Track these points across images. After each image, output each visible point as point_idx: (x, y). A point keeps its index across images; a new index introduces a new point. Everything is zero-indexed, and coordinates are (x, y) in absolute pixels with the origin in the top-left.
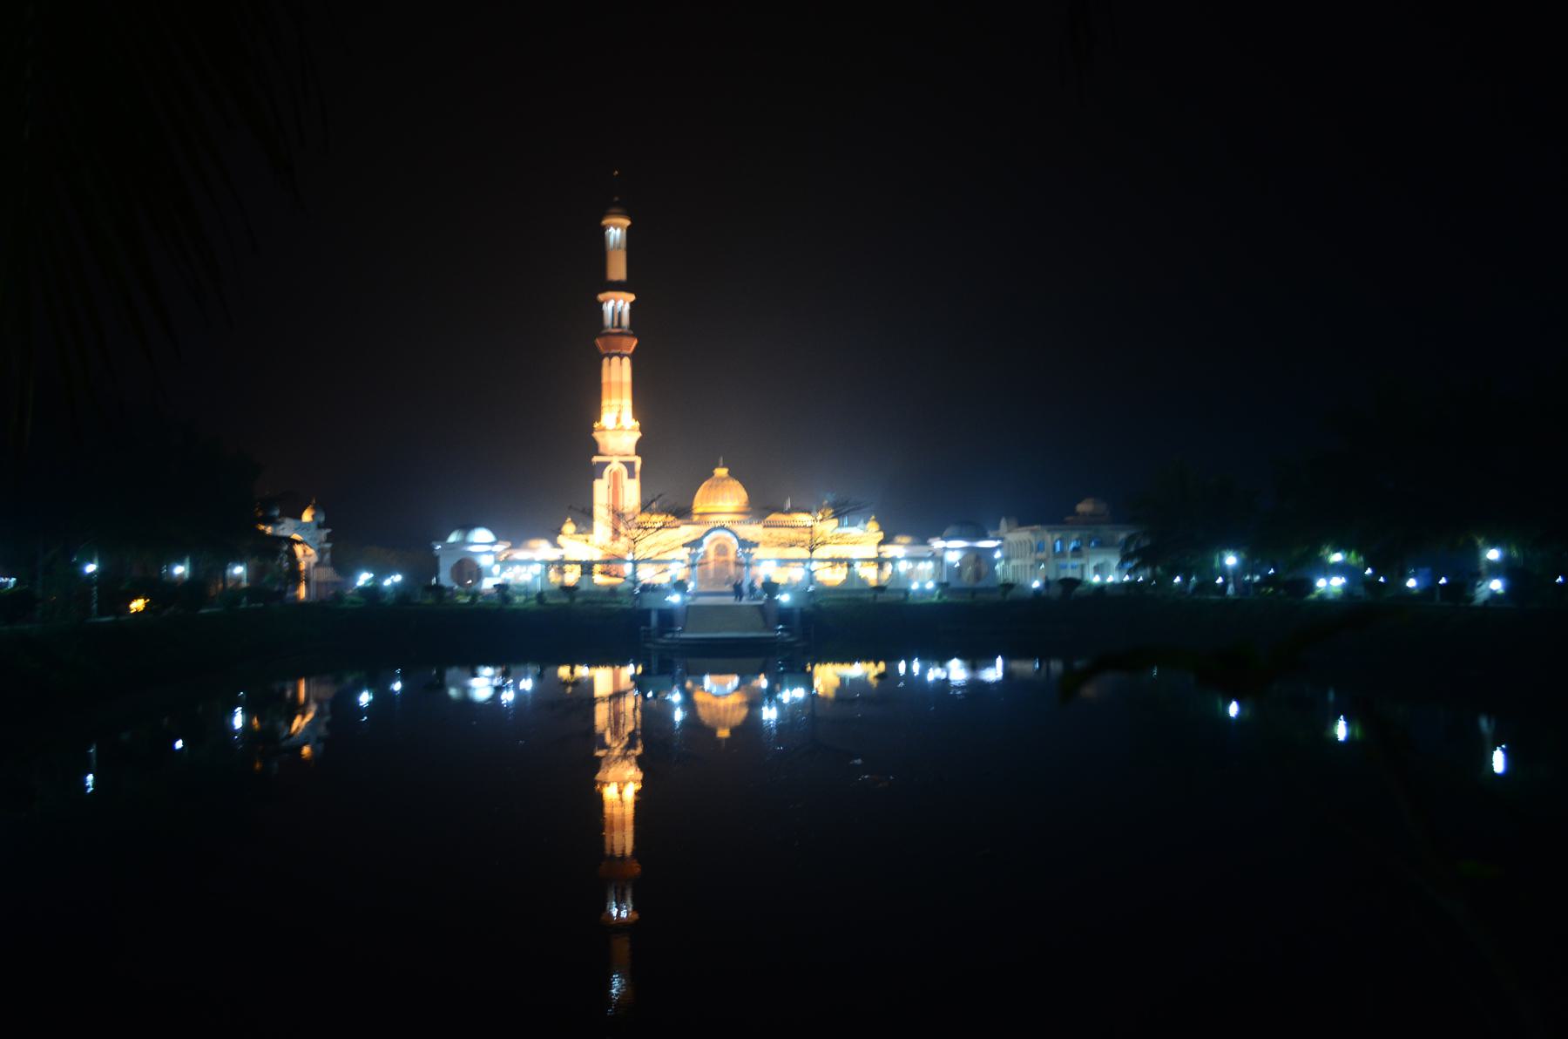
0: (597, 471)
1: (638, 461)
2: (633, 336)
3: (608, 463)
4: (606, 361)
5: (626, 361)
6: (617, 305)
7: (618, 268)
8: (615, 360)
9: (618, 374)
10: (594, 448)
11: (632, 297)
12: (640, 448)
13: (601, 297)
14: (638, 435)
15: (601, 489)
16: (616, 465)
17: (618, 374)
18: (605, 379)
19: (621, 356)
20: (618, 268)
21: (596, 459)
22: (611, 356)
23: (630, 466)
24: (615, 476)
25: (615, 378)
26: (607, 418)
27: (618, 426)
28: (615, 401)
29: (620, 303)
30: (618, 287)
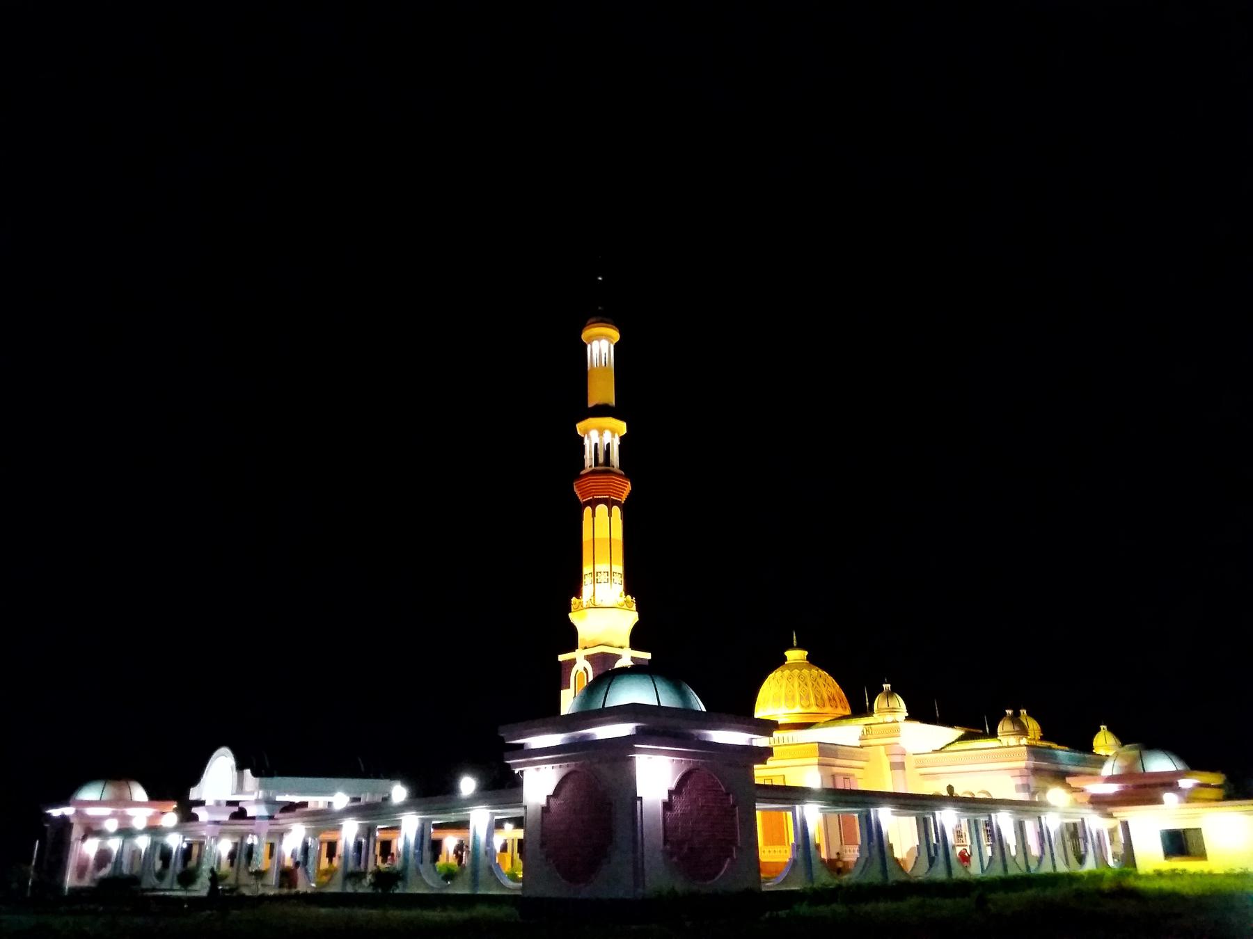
2: (627, 476)
4: (588, 510)
5: (616, 510)
6: (602, 436)
8: (602, 509)
9: (603, 530)
11: (622, 427)
13: (580, 427)
14: (633, 617)
17: (603, 530)
19: (610, 503)
22: (593, 504)
25: (602, 533)
29: (607, 434)
30: (602, 411)
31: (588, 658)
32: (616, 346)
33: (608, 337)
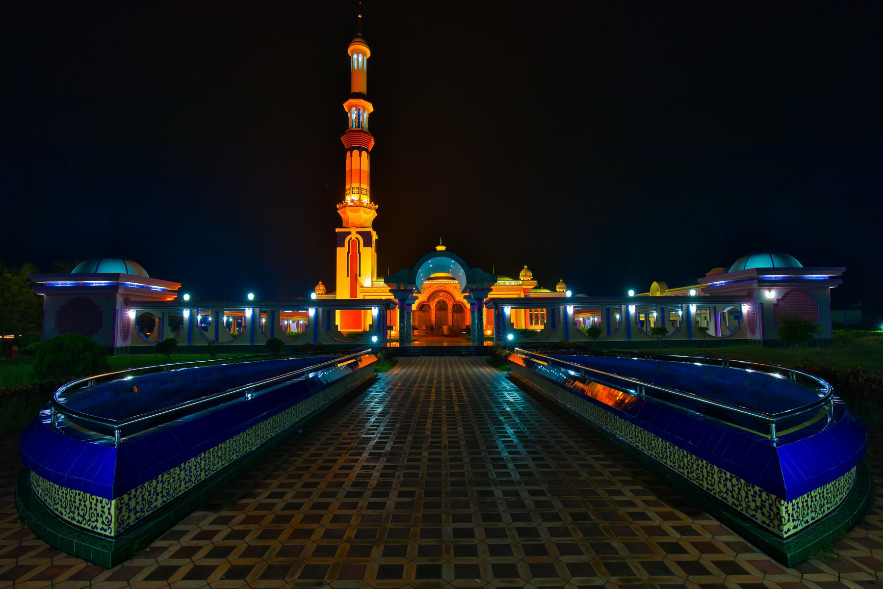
0: (339, 240)
1: (375, 237)
2: (373, 135)
3: (350, 233)
4: (349, 153)
5: (364, 154)
6: (358, 112)
7: (360, 84)
8: (356, 153)
9: (359, 163)
10: (339, 222)
12: (376, 224)
15: (342, 254)
16: (354, 235)
17: (359, 163)
18: (348, 169)
19: (361, 150)
20: (360, 84)
21: (337, 230)
22: (351, 149)
23: (366, 236)
24: (354, 244)
25: (355, 166)
26: (348, 199)
27: (359, 207)
28: (355, 185)
30: (359, 96)
31: (358, 233)
32: (368, 60)
33: (364, 55)
